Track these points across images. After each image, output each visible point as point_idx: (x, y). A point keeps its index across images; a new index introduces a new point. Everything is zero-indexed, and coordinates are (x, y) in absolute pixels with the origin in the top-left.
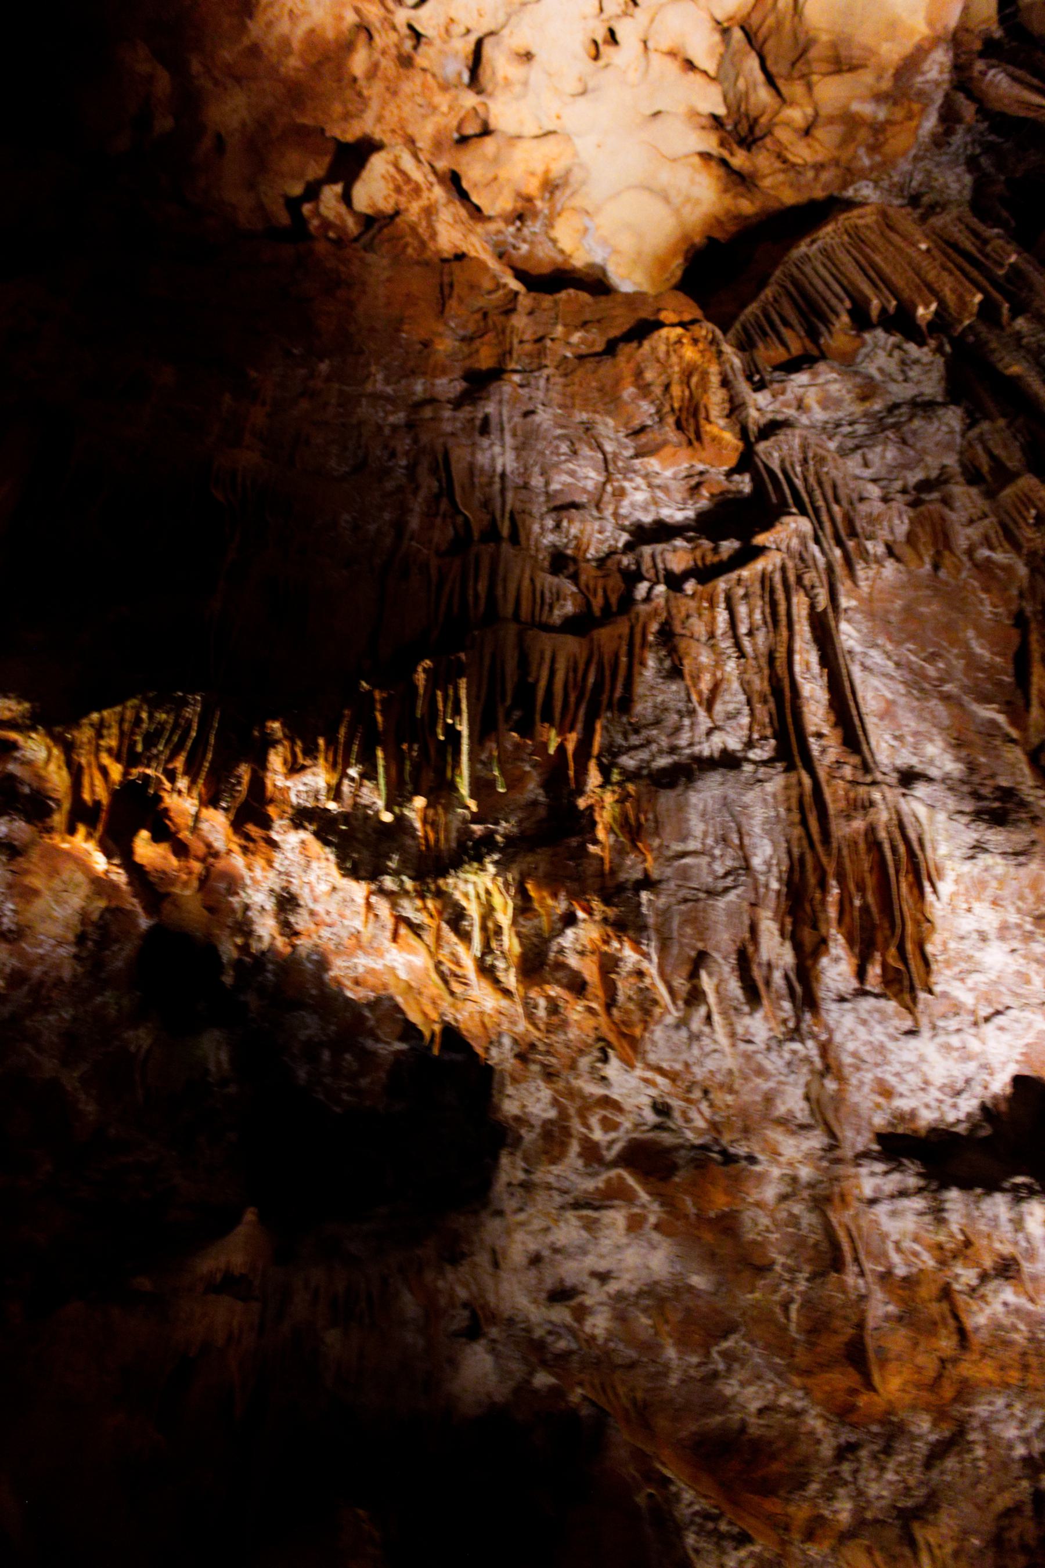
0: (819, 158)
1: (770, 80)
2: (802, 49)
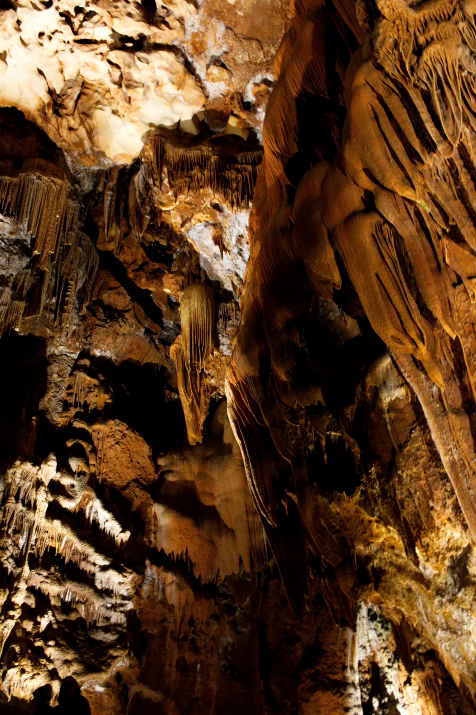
0: (67, 139)
1: (76, 102)
2: (87, 115)
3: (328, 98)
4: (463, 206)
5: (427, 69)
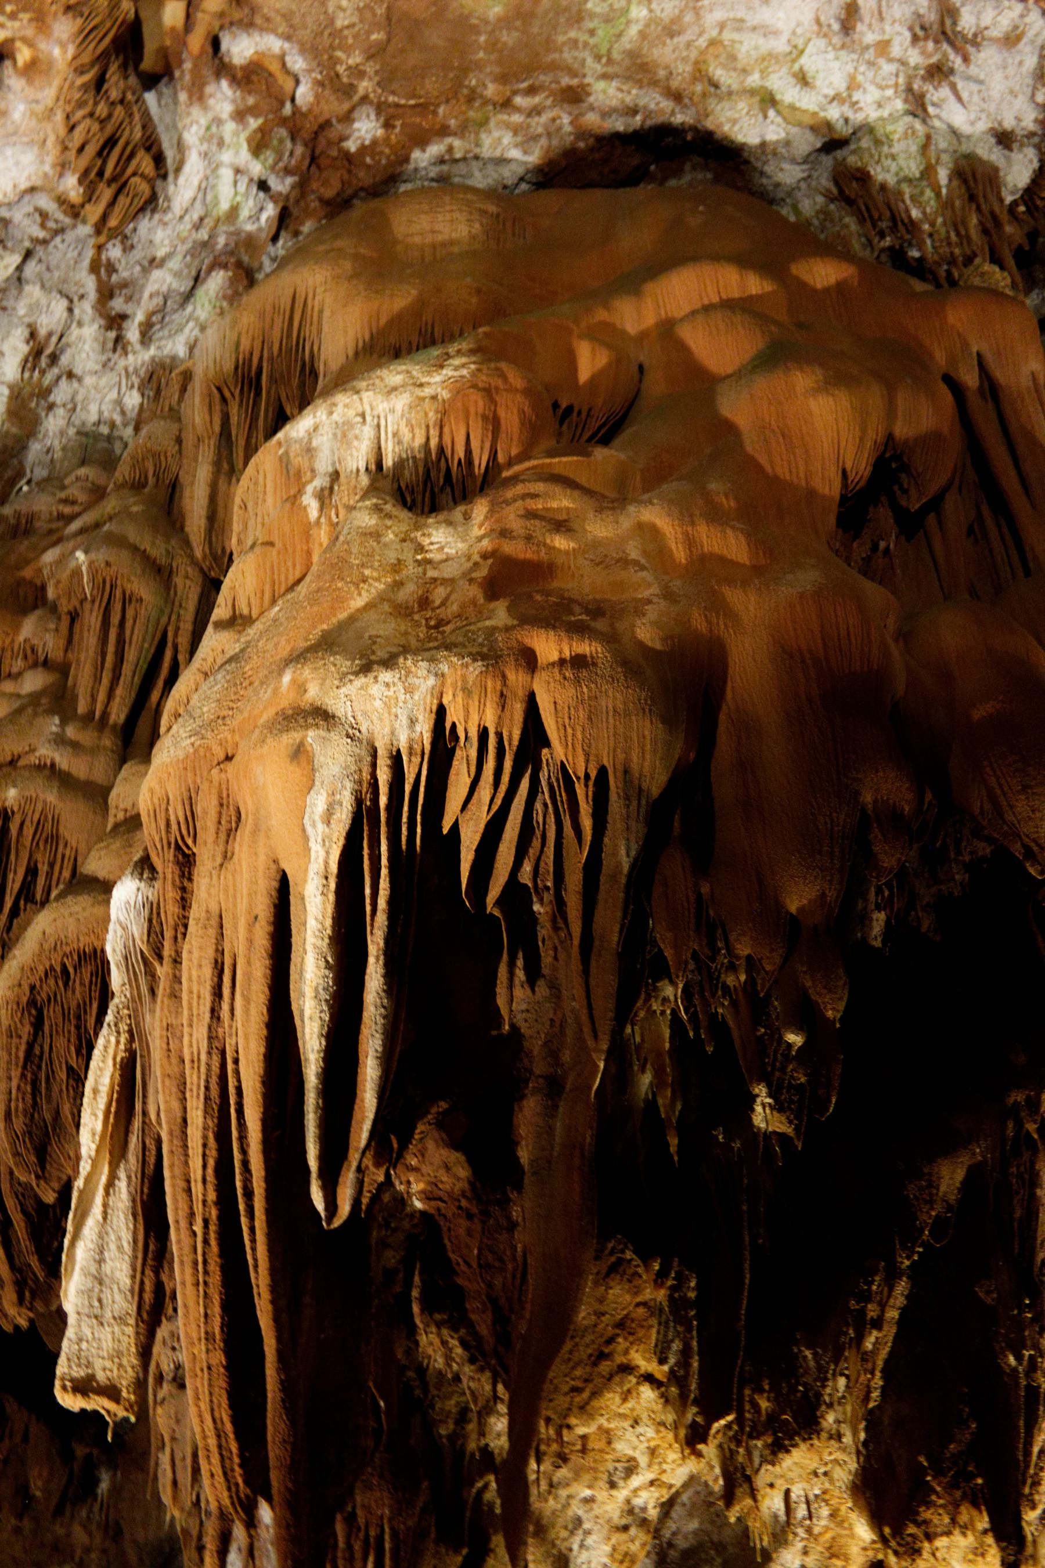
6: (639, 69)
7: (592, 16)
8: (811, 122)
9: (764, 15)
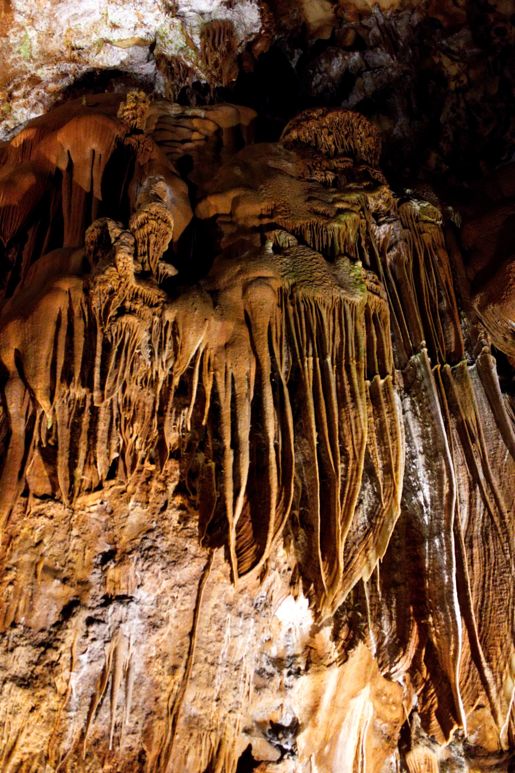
3: (5, 245)
4: (69, 437)
5: (120, 328)
6: (49, 58)
7: (14, 45)
8: (134, 43)
9: (84, 6)
